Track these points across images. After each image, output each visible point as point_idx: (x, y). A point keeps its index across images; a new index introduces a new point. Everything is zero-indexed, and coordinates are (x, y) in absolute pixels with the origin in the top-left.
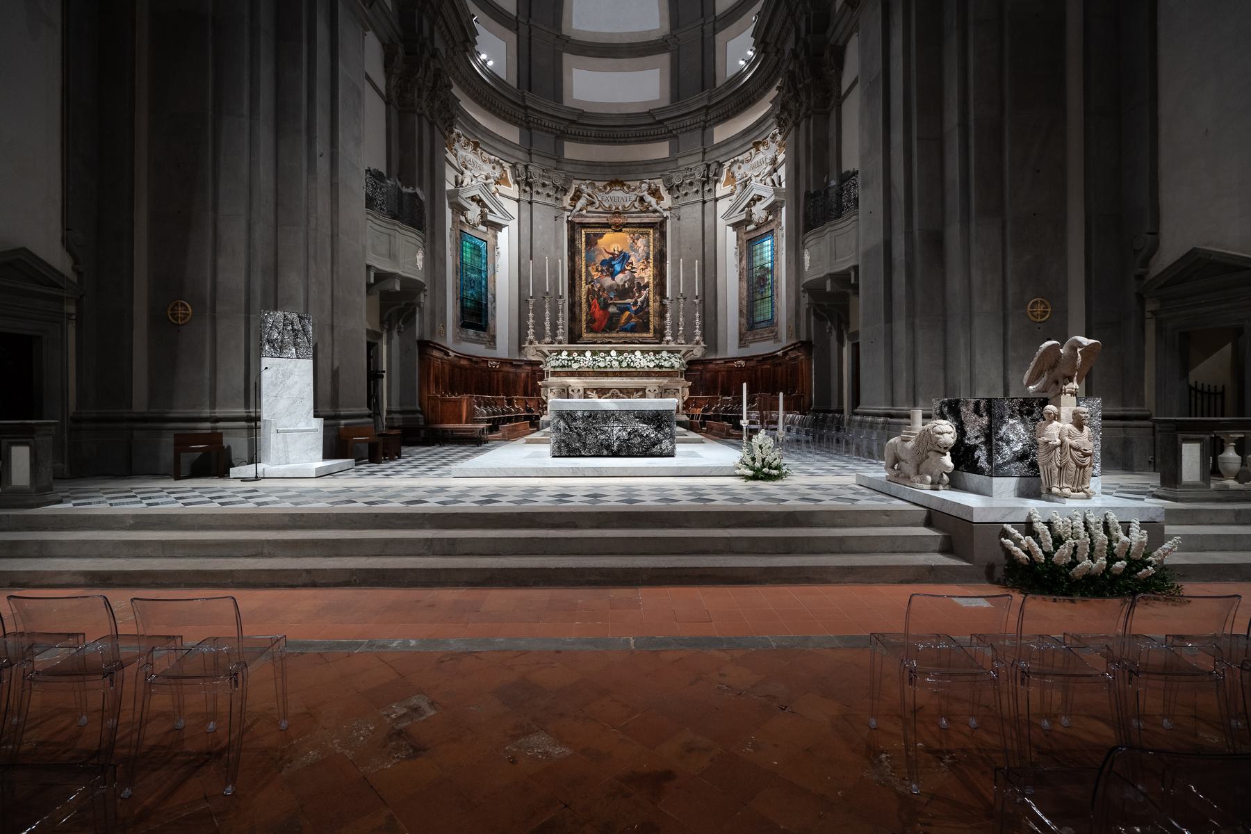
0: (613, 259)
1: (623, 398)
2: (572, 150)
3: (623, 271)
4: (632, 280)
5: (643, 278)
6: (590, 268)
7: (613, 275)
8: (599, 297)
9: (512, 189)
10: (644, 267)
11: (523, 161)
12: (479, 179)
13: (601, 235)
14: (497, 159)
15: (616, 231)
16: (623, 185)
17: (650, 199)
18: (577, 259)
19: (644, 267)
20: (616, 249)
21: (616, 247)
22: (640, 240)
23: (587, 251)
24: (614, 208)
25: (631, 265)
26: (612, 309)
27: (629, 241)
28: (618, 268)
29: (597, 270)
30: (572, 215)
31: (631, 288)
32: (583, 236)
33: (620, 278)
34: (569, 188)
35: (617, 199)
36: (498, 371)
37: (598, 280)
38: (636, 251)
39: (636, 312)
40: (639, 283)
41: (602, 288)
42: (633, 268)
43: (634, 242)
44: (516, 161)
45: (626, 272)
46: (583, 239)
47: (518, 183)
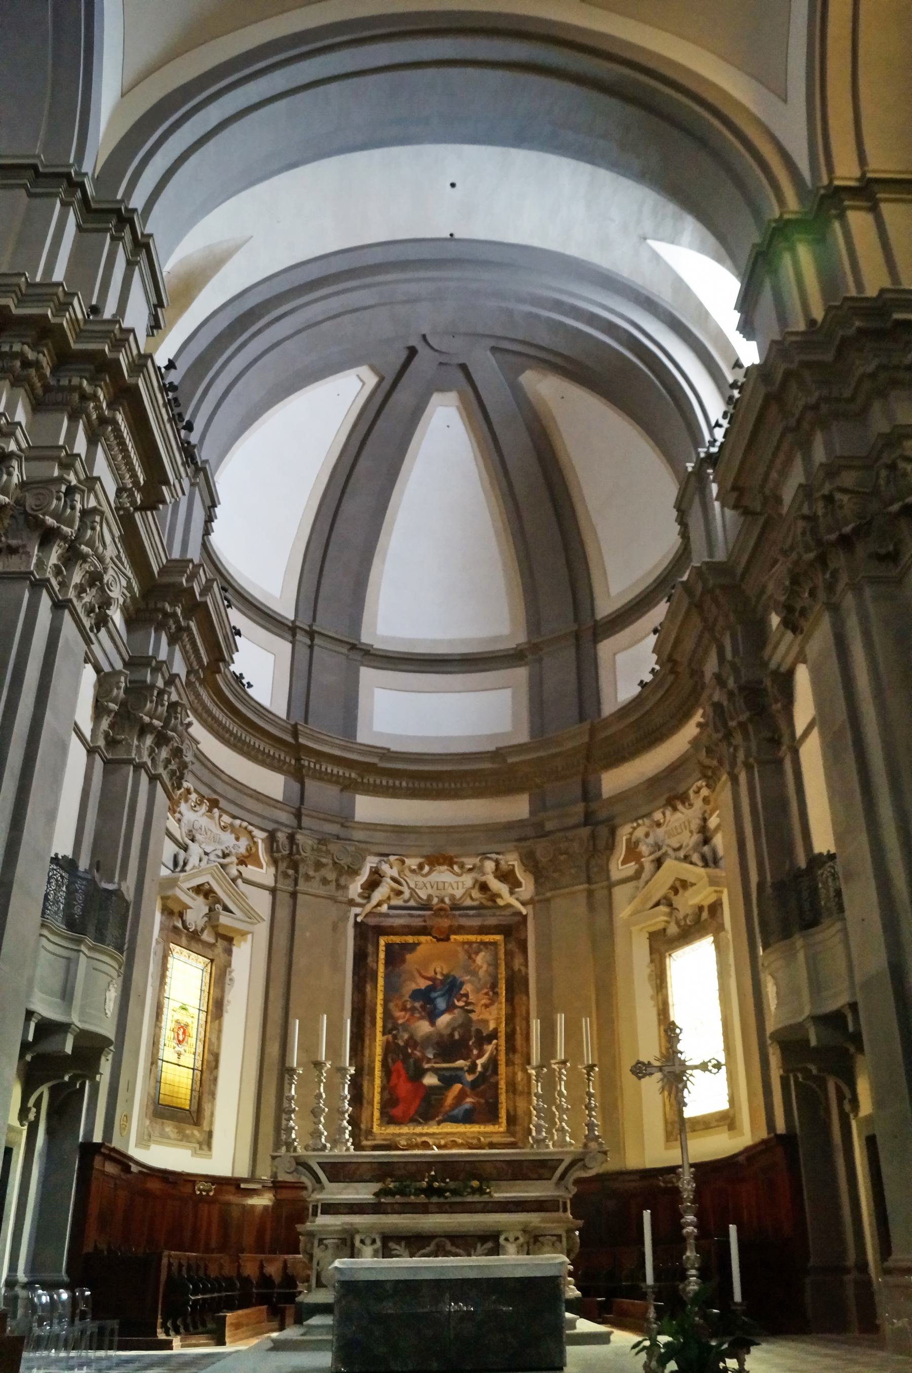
0: (431, 989)
1: (457, 1255)
3: (450, 1008)
4: (466, 1024)
6: (391, 1005)
7: (432, 1017)
8: (407, 1056)
9: (264, 871)
10: (488, 1002)
11: (287, 826)
12: (212, 857)
13: (413, 947)
14: (245, 824)
15: (439, 940)
16: (451, 865)
17: (496, 885)
18: (368, 988)
19: (488, 1002)
20: (438, 970)
21: (439, 969)
22: (482, 954)
23: (387, 977)
24: (435, 901)
25: (464, 999)
26: (430, 1080)
27: (462, 955)
28: (441, 1004)
29: (404, 1009)
30: (364, 915)
31: (464, 1039)
32: (382, 948)
33: (444, 1020)
34: (360, 869)
35: (441, 886)
36: (212, 1201)
37: (405, 1027)
39: (474, 1085)
40: (479, 1032)
41: (412, 1042)
42: (468, 1004)
43: (470, 957)
44: (275, 826)
45: (456, 1011)
46: (382, 955)
47: (275, 862)
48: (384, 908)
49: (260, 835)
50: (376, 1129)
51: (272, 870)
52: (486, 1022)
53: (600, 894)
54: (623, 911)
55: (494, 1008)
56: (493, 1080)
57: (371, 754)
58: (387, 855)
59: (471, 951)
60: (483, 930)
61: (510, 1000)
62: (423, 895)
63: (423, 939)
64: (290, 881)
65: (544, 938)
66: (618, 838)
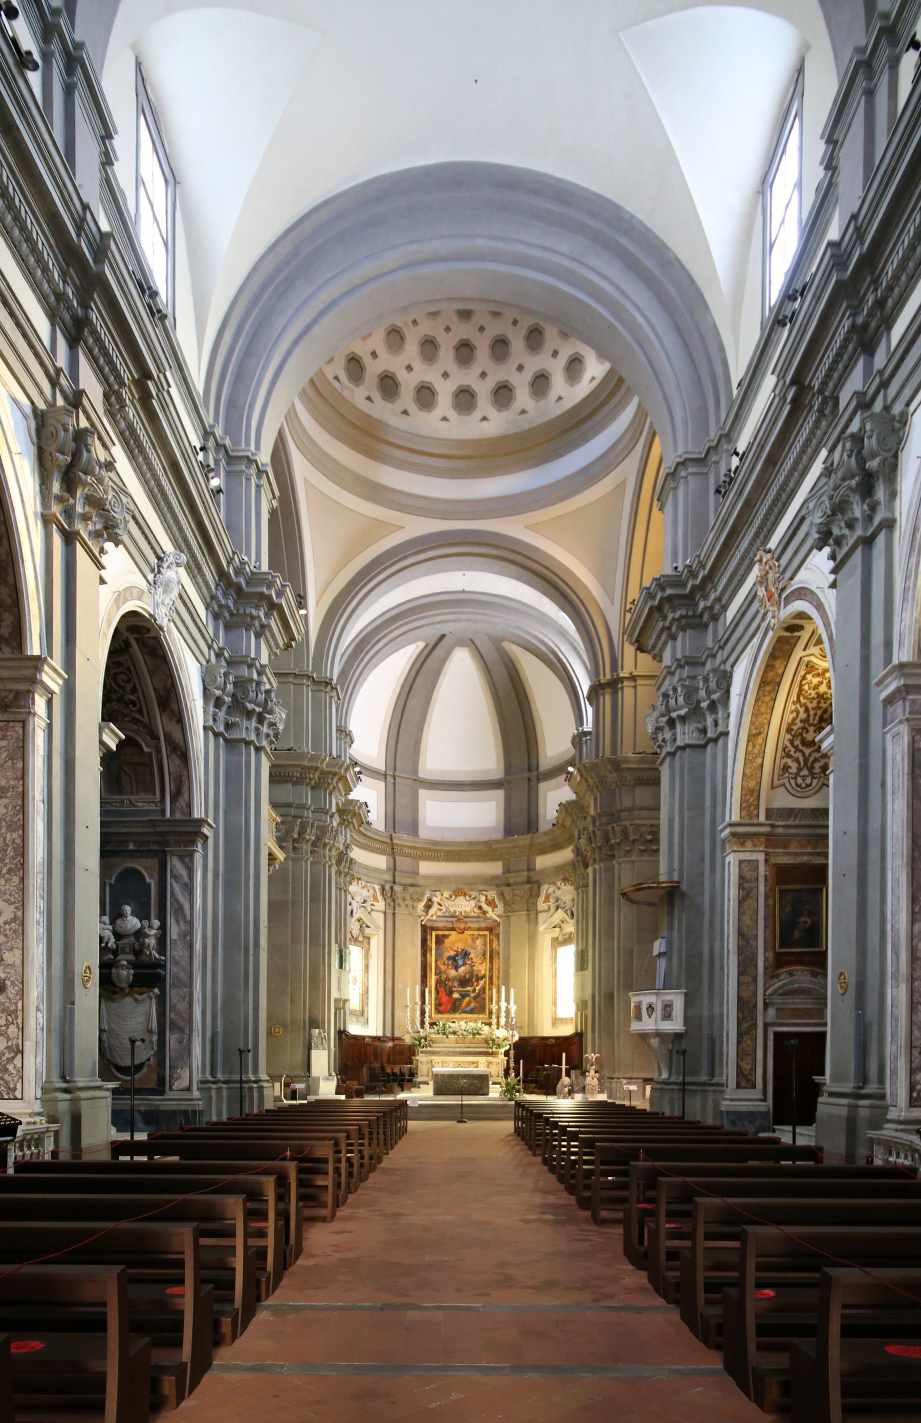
0: (457, 955)
2: (426, 868)
3: (465, 964)
4: (472, 972)
5: (480, 971)
8: (445, 985)
13: (446, 936)
16: (465, 895)
18: (428, 955)
21: (460, 946)
22: (478, 940)
26: (456, 996)
27: (470, 940)
28: (460, 962)
29: (444, 964)
37: (445, 972)
38: (475, 949)
39: (475, 998)
41: (448, 979)
46: (434, 940)
48: (434, 918)
49: (377, 887)
50: (433, 1015)
51: (384, 903)
52: (480, 971)
53: (533, 916)
54: (541, 928)
55: (484, 965)
56: (483, 996)
57: (427, 843)
58: (435, 891)
59: (474, 939)
60: (479, 929)
61: (491, 962)
62: (452, 910)
63: (452, 933)
64: (391, 908)
65: (508, 933)
66: (541, 890)
